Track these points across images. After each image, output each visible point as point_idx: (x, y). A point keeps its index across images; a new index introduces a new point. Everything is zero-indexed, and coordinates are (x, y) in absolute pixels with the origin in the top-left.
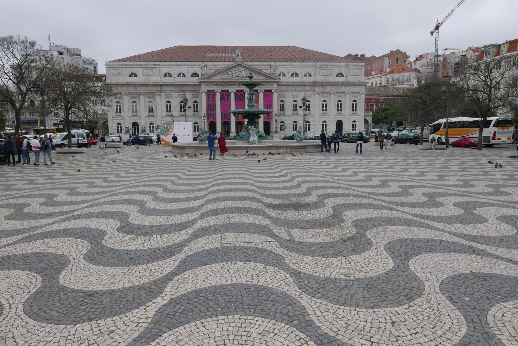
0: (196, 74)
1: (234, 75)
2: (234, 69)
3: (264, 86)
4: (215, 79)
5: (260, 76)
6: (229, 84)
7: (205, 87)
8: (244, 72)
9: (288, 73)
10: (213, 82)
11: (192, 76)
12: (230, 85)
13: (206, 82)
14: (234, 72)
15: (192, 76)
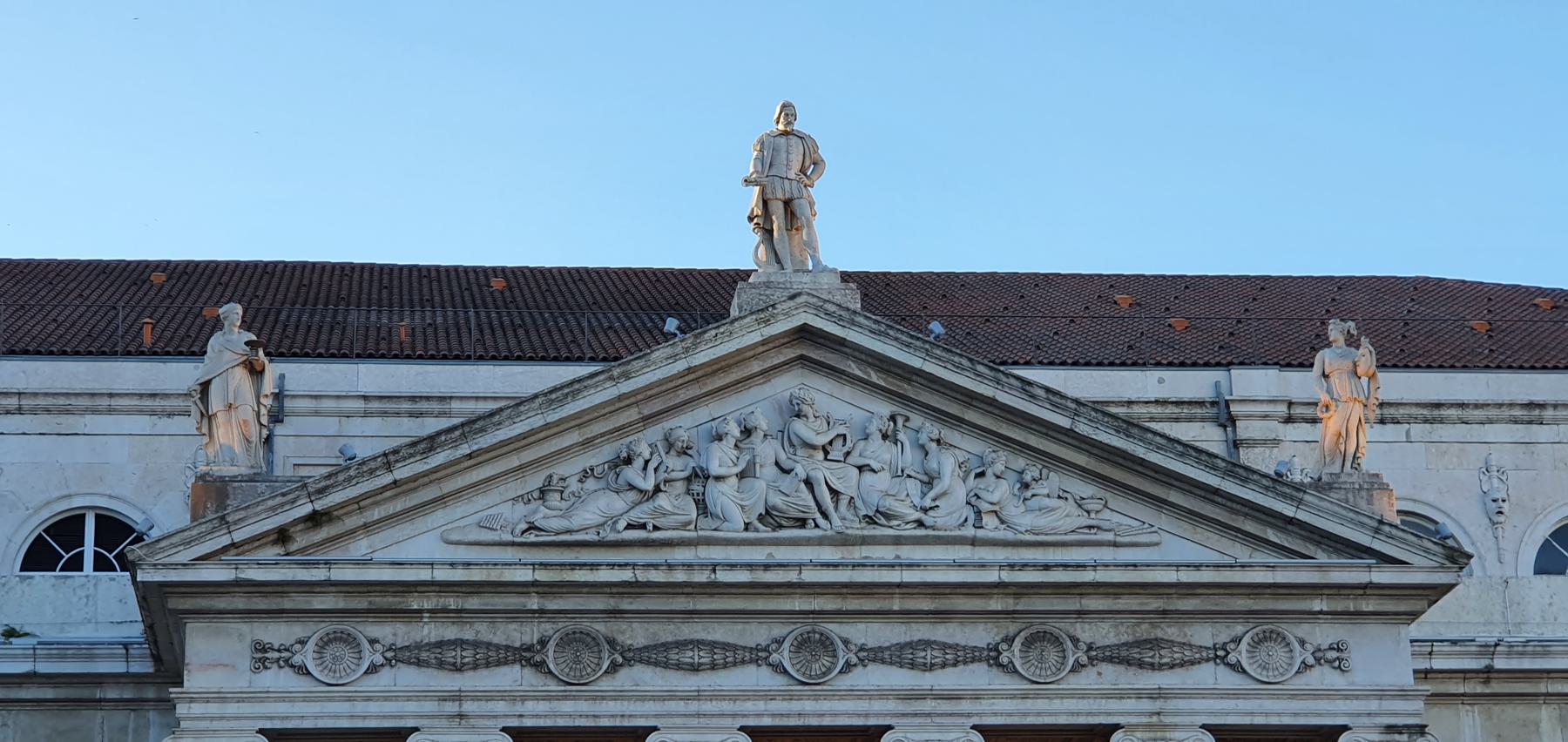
0: (114, 530)
1: (724, 496)
2: (730, 411)
3: (1208, 675)
4: (419, 547)
5: (1123, 515)
6: (636, 634)
7: (242, 679)
8: (878, 452)
9: (1495, 513)
10: (389, 599)
11: (38, 557)
12: (656, 655)
13: (268, 601)
14: (721, 459)
15: (38, 557)
